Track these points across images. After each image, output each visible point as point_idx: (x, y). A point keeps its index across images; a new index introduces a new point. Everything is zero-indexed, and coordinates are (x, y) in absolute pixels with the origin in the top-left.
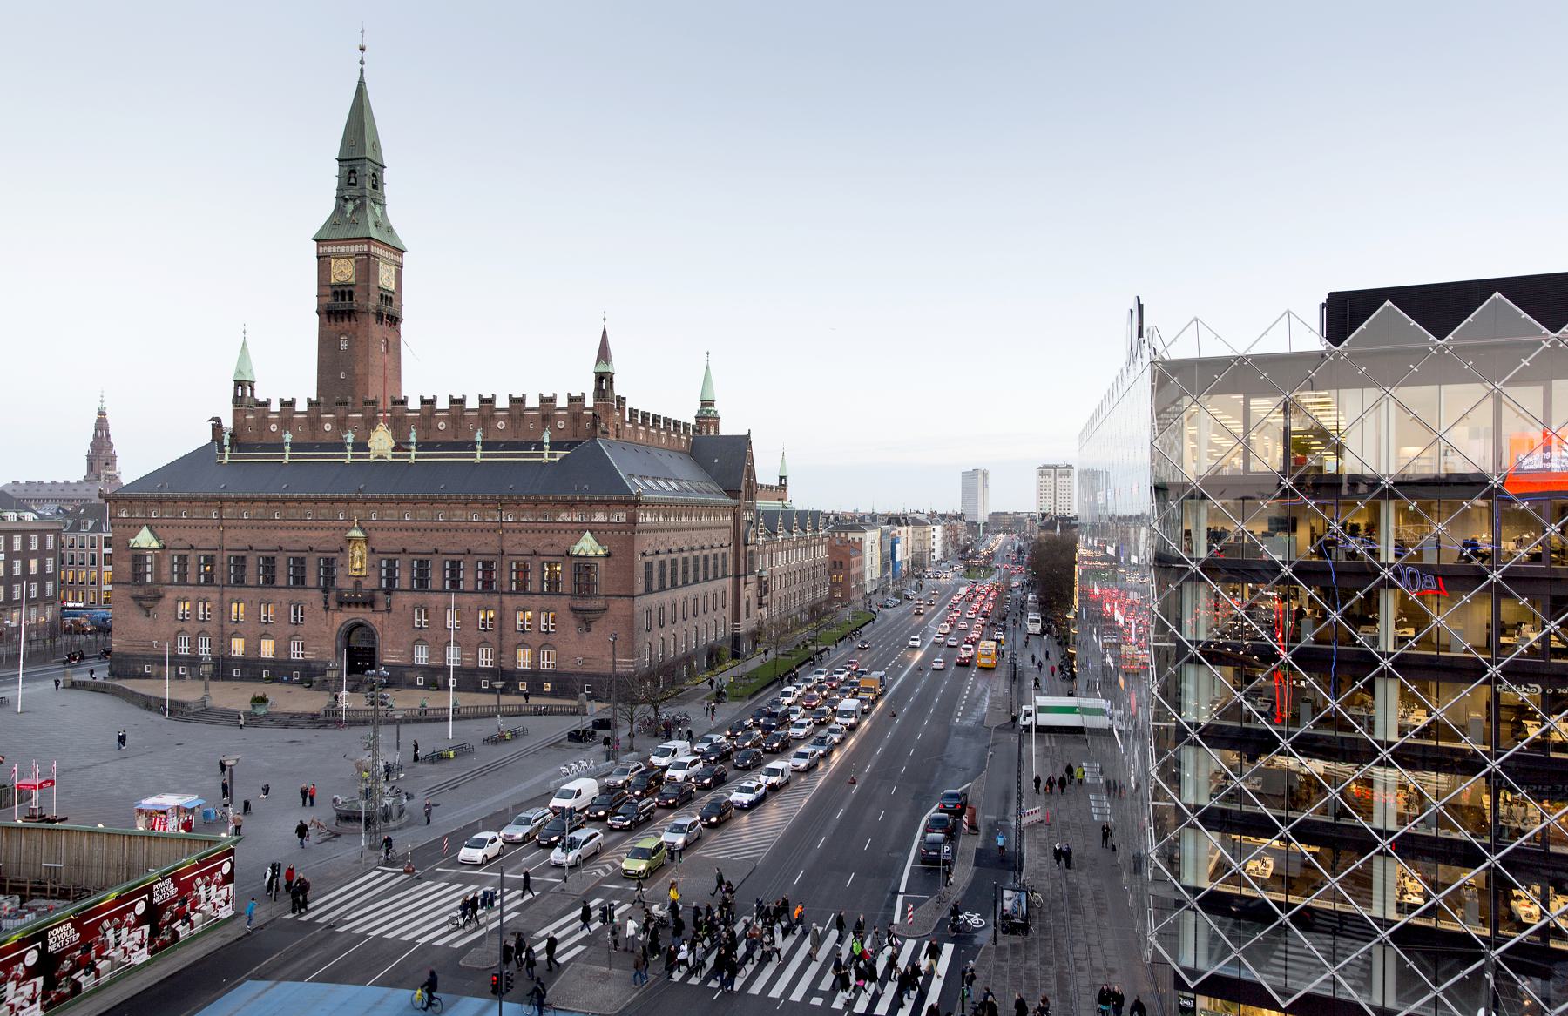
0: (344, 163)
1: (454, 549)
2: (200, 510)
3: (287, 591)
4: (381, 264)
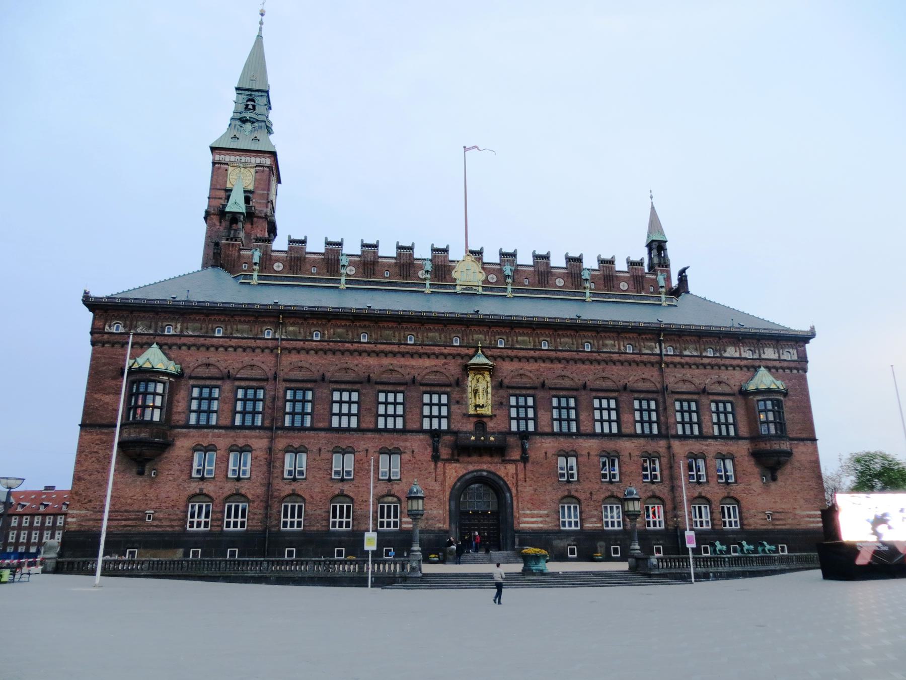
0: (240, 92)
2: (246, 327)
3: (377, 436)
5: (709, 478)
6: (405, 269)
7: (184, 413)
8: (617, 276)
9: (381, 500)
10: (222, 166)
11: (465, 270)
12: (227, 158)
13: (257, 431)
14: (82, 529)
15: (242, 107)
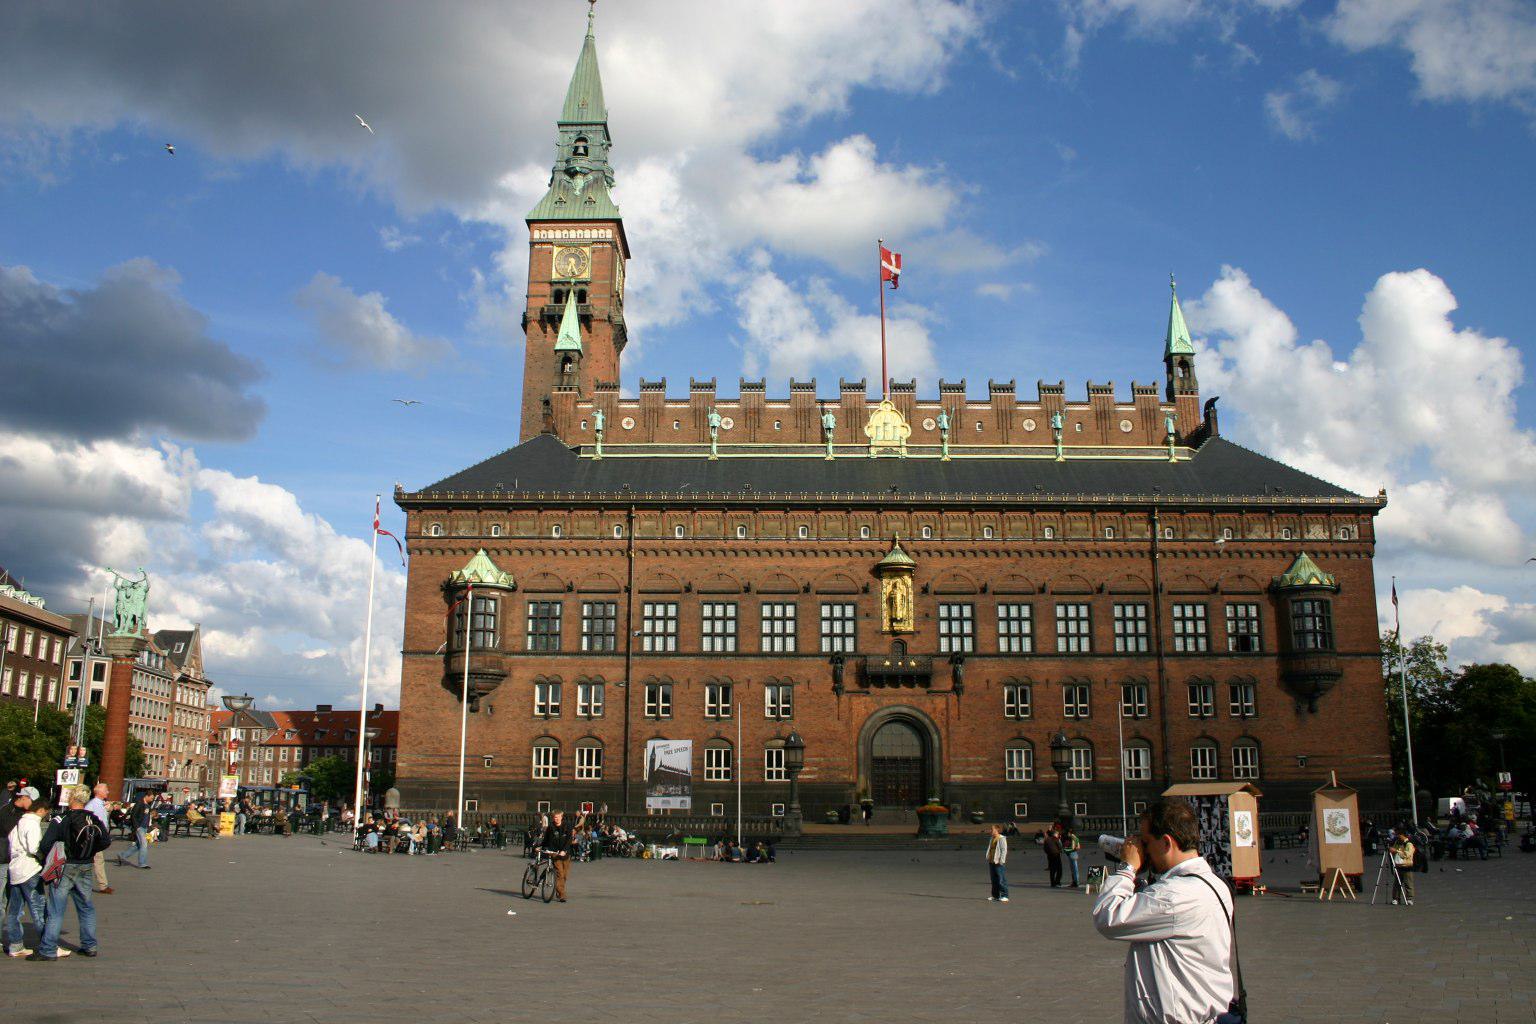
0: (565, 128)
1: (1072, 585)
2: (590, 524)
5: (1219, 711)
6: (803, 419)
7: (520, 635)
8: (1115, 412)
9: (768, 744)
10: (545, 247)
11: (881, 425)
12: (551, 235)
13: (610, 657)
14: (415, 775)
15: (567, 152)
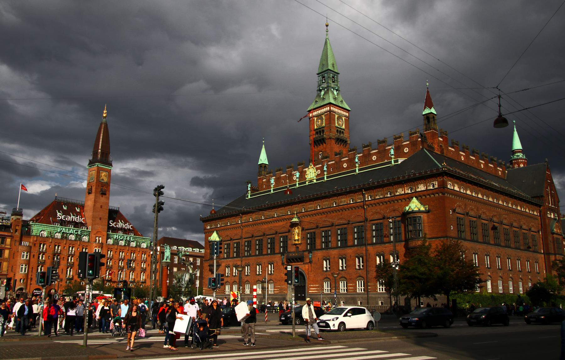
0: (319, 75)
4: (336, 116)
